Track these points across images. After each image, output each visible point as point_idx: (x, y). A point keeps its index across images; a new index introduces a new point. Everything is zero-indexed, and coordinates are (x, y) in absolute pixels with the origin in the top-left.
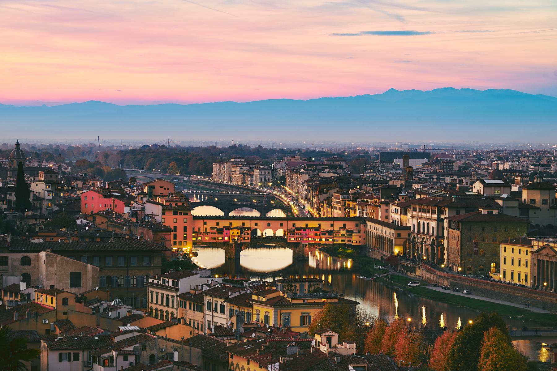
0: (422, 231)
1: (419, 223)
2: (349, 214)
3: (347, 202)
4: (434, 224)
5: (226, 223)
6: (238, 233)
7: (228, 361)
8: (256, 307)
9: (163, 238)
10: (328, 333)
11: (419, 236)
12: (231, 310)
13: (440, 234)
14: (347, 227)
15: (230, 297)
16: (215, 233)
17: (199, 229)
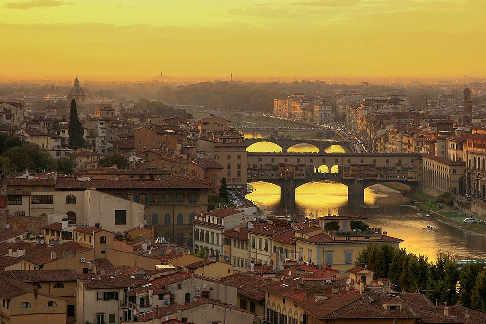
0: (477, 167)
2: (406, 150)
3: (404, 138)
6: (293, 169)
7: (264, 300)
8: (299, 245)
11: (475, 172)
12: (275, 248)
16: (269, 170)
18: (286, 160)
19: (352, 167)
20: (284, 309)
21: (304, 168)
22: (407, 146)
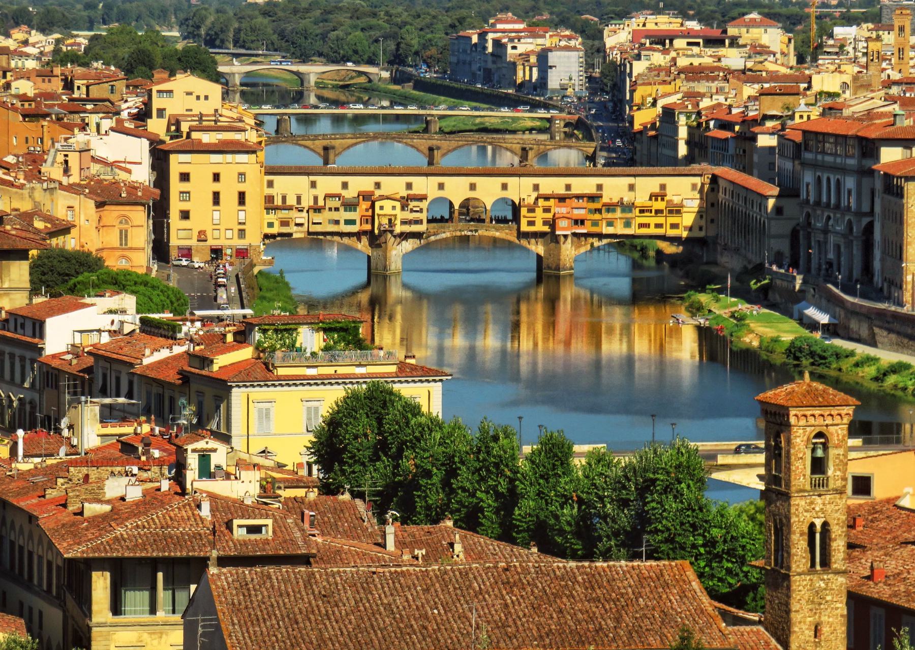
0: (824, 199)
1: (819, 180)
4: (850, 183)
5: (364, 184)
6: (394, 208)
9: (126, 220)
10: (201, 445)
11: (819, 212)
13: (866, 208)
14: (669, 191)
15: (146, 361)
16: (337, 209)
17: (299, 199)
18: (378, 185)
19: (541, 202)
20: (31, 537)
21: (424, 205)
22: (697, 151)
